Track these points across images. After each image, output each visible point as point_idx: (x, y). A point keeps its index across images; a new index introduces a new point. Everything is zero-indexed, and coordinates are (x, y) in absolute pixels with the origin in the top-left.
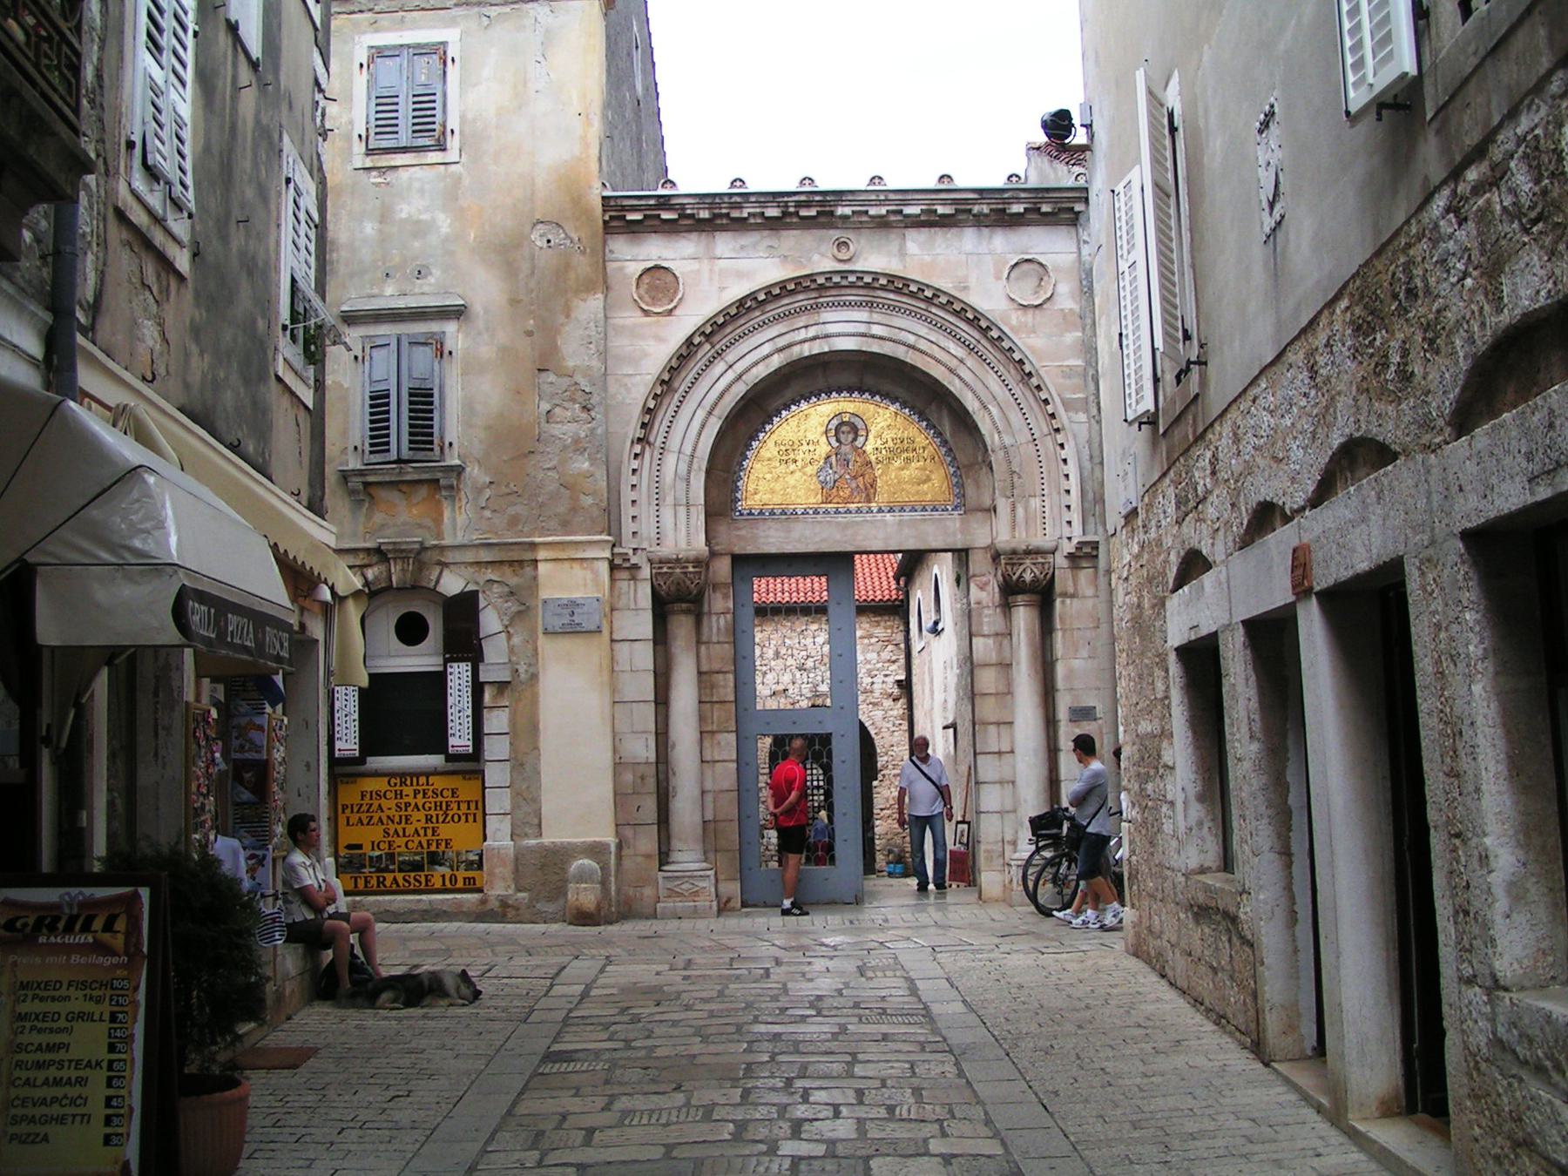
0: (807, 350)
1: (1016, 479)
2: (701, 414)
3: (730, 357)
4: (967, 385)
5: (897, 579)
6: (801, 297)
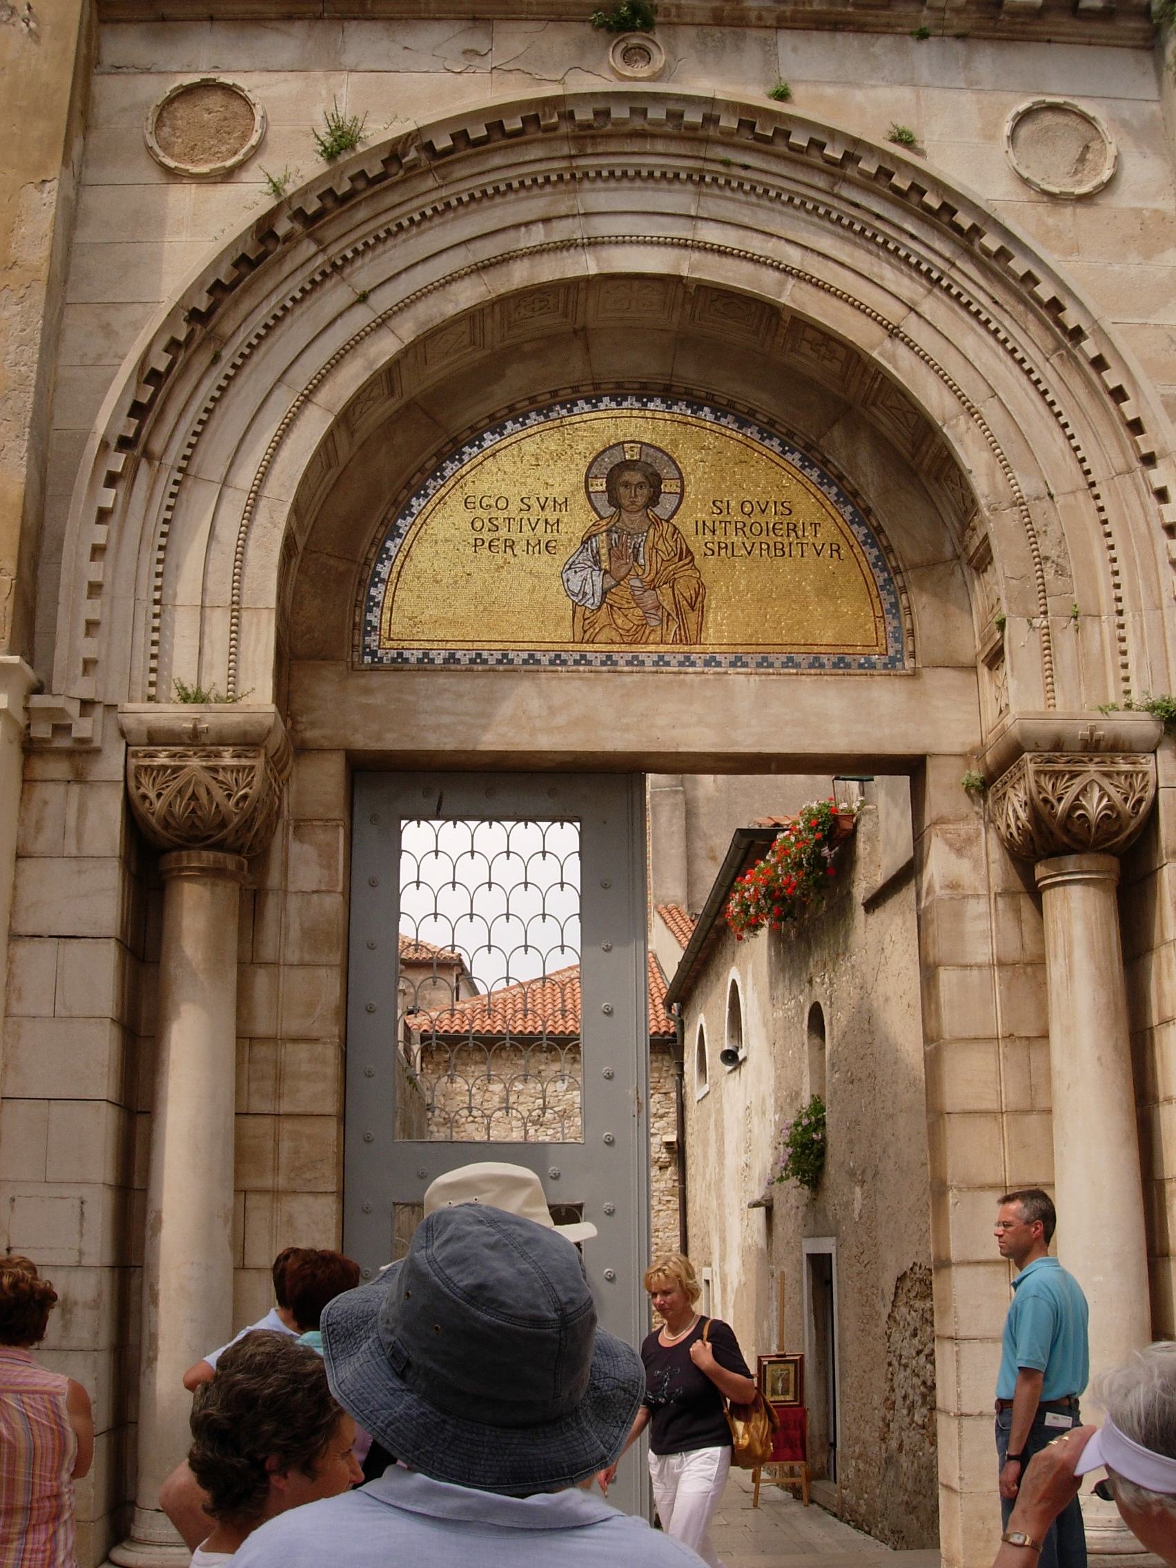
0: (550, 270)
1: (1050, 575)
2: (284, 400)
3: (364, 275)
4: (924, 358)
5: (668, 1006)
6: (535, 152)
